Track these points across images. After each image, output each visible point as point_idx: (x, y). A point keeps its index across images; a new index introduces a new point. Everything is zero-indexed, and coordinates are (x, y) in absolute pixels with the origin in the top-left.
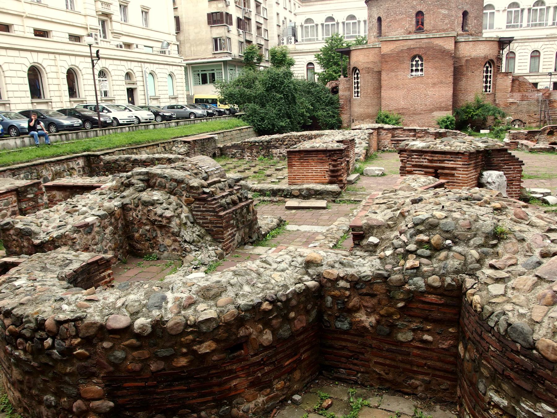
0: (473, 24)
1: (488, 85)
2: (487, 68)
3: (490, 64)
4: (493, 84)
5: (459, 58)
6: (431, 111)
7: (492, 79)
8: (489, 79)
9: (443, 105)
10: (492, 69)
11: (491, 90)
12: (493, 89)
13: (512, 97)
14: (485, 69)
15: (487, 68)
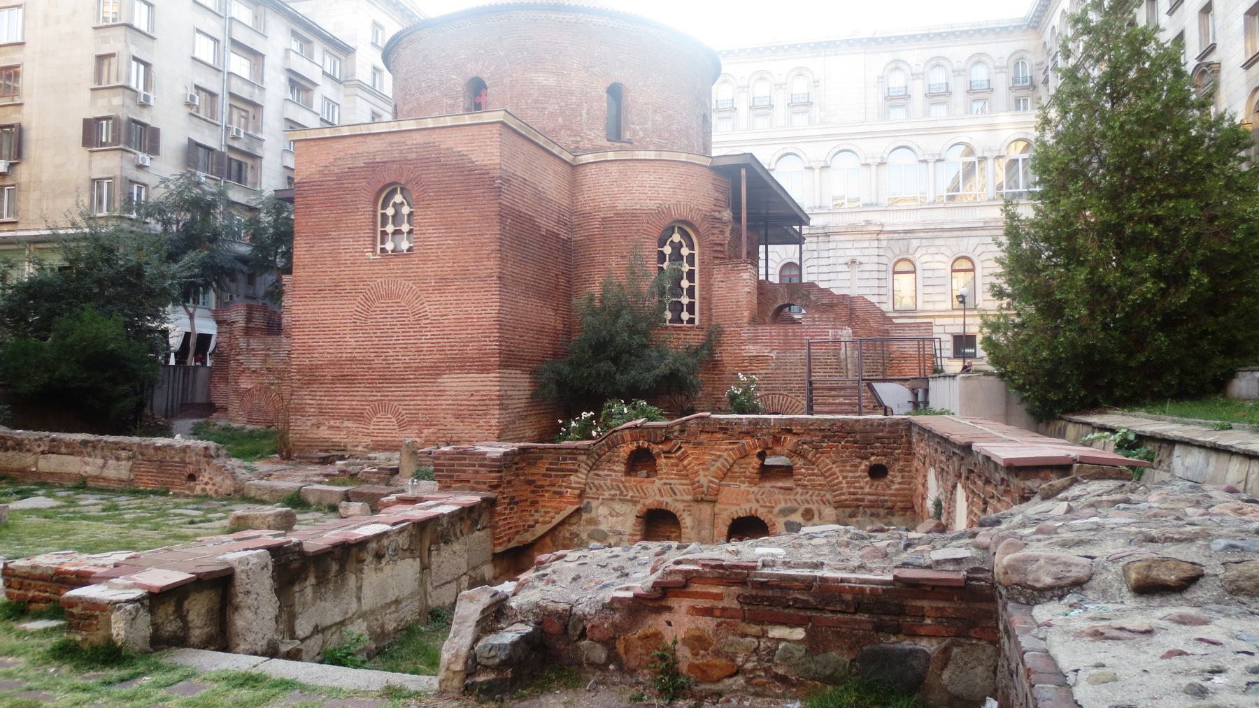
0: (649, 125)
1: (685, 300)
2: (677, 248)
3: (685, 234)
4: (702, 298)
5: (584, 215)
6: (436, 371)
7: (697, 284)
8: (685, 284)
9: (471, 350)
10: (696, 252)
11: (697, 316)
12: (701, 314)
13: (754, 340)
14: (667, 250)
15: (677, 248)
